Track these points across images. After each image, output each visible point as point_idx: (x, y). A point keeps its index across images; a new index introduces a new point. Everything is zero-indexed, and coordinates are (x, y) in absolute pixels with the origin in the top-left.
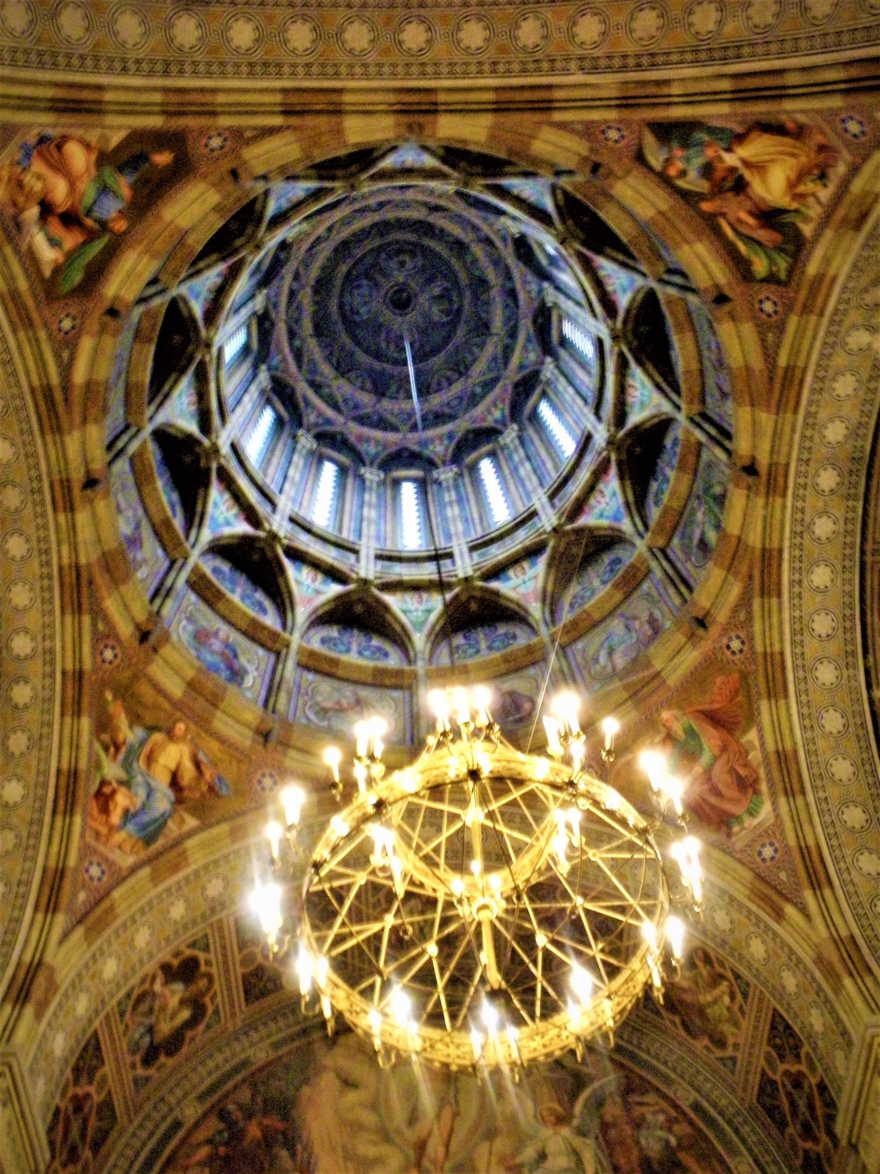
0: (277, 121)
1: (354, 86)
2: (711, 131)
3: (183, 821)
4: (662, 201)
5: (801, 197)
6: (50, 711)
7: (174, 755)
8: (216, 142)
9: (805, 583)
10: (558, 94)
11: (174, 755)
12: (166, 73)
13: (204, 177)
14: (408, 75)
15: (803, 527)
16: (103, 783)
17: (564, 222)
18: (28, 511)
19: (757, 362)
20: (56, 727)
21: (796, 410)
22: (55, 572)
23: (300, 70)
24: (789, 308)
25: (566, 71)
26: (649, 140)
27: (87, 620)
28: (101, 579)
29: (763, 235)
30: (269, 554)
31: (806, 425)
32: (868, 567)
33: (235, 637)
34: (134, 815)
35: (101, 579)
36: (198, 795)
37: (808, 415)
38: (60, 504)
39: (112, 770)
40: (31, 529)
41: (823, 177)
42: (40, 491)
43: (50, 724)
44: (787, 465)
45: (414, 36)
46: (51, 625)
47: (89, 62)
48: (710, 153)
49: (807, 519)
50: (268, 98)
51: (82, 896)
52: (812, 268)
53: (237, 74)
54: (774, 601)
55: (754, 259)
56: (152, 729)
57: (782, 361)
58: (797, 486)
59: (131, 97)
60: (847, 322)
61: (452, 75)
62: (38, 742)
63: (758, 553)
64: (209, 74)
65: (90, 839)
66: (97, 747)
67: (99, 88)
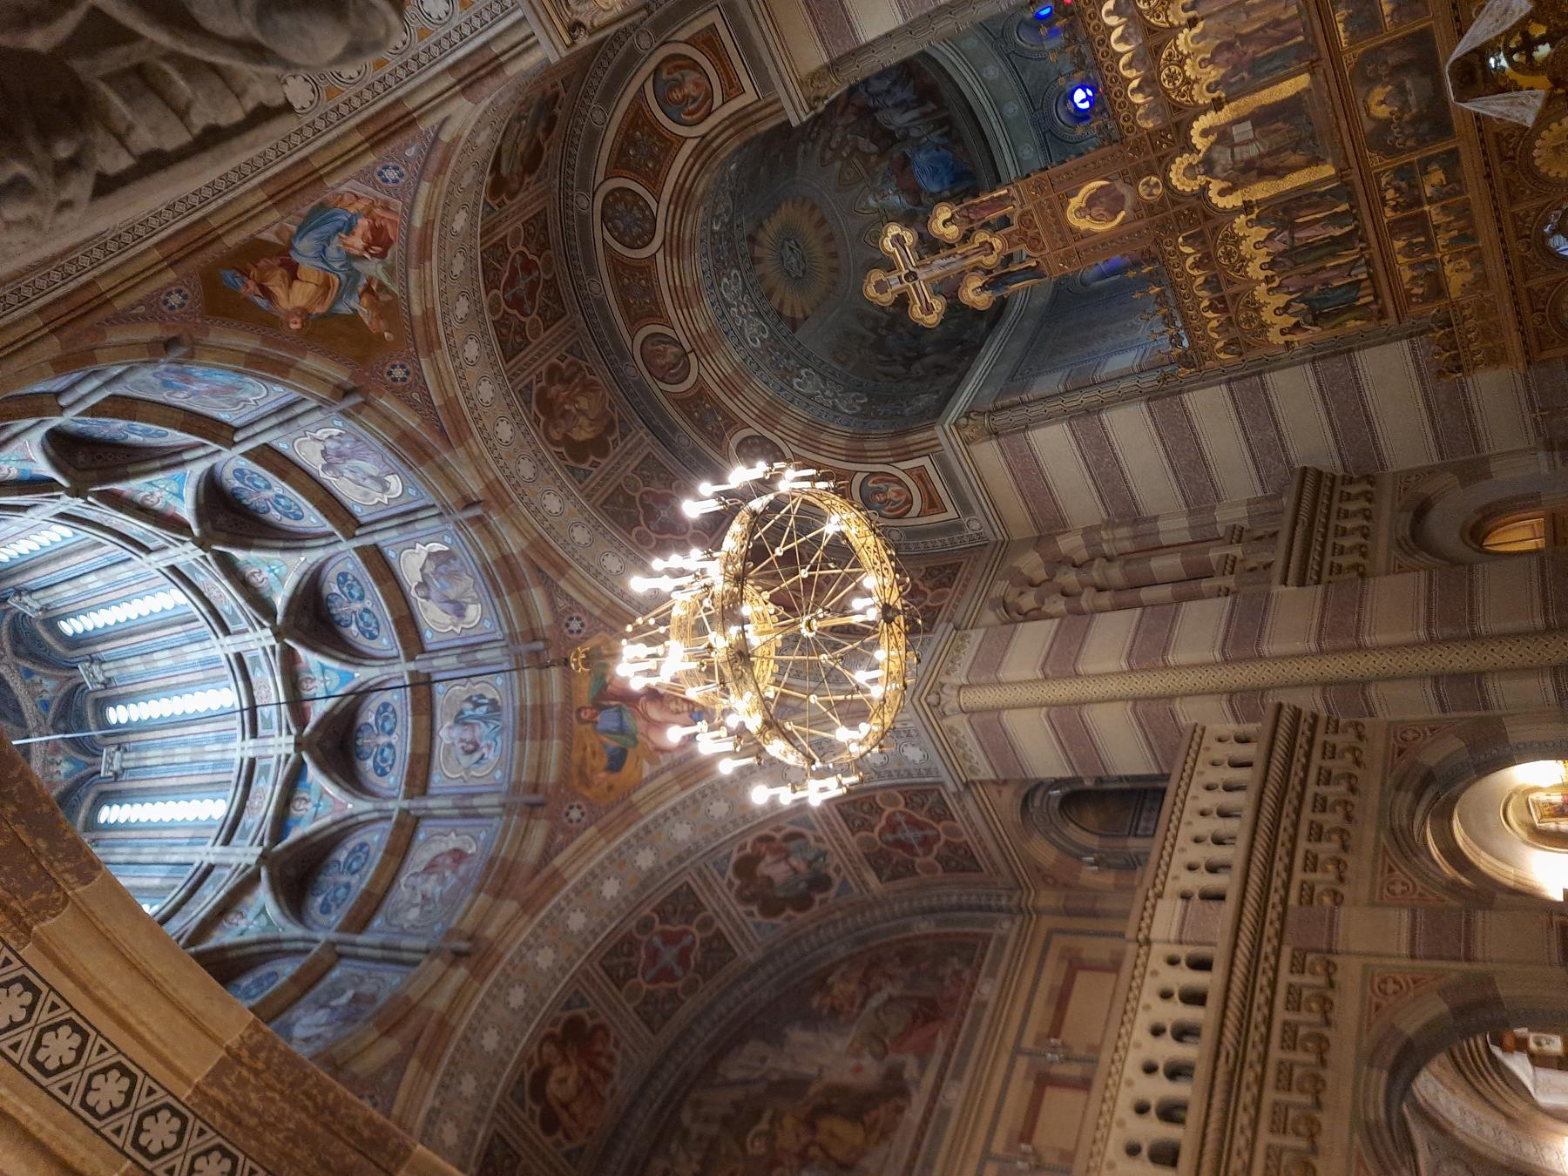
0: (558, 861)
1: (526, 929)
3: (277, 234)
6: (442, 303)
7: (296, 297)
8: (575, 814)
11: (296, 297)
12: (646, 829)
13: (557, 786)
16: (382, 255)
18: (512, 465)
20: (437, 293)
22: (473, 426)
23: (563, 903)
25: (437, 1094)
27: (437, 401)
28: (426, 436)
30: (71, 471)
33: (163, 396)
34: (340, 230)
35: (426, 436)
36: (262, 263)
38: (497, 486)
39: (373, 268)
40: (503, 451)
42: (514, 488)
43: (442, 293)
45: (517, 997)
46: (461, 379)
47: (699, 797)
50: (572, 869)
51: (410, 152)
53: (601, 865)
56: (331, 315)
59: (661, 798)
61: (483, 1005)
62: (446, 270)
64: (618, 850)
65: (398, 205)
66: (395, 289)
67: (683, 789)
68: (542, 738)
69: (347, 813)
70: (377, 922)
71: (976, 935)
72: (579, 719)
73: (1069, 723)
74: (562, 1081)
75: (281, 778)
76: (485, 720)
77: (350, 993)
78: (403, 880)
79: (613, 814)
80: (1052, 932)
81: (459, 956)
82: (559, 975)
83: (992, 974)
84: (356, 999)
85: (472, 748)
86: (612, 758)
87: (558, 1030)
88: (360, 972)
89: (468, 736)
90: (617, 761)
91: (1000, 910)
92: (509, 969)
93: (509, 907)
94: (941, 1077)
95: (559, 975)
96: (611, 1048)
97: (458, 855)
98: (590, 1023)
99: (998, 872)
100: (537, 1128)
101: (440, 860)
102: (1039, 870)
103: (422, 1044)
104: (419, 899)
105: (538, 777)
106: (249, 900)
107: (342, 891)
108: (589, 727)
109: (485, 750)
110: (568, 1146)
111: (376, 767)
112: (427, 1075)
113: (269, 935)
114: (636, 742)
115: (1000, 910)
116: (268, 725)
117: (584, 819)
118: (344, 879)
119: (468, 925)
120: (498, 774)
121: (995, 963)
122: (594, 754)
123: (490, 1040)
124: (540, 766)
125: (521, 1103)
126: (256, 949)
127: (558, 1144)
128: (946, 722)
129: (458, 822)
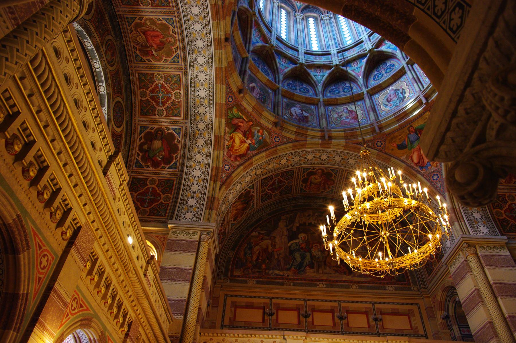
2: (255, 149)
4: (263, 121)
5: (231, 139)
8: (379, 144)
9: (202, 9)
10: (291, 149)
13: (385, 134)
14: (327, 151)
15: (206, 27)
17: (273, 54)
19: (230, 80)
21: (216, 68)
24: (226, 102)
25: (289, 153)
26: (268, 140)
29: (236, 121)
31: (212, 63)
32: (175, 8)
37: (212, 67)
41: (228, 148)
44: (215, 49)
45: (324, 157)
48: (254, 141)
49: (205, 30)
52: (223, 120)
54: (213, 3)
55: (237, 112)
57: (224, 86)
58: (211, 42)
60: (208, 100)
61: (316, 150)
63: (222, 19)
68: (397, 121)
69: (358, 78)
70: (330, 108)
71: (409, 280)
72: (409, 128)
73: (476, 297)
74: (316, 179)
75: (359, 53)
76: (399, 98)
77: (308, 115)
78: (345, 106)
79: (384, 155)
80: (418, 305)
81: (323, 137)
82: (336, 164)
83: (396, 289)
84: (306, 117)
85: (389, 100)
86: (402, 145)
87: (325, 171)
88: (315, 114)
89: (392, 96)
90: (401, 147)
91: (420, 286)
92: (329, 152)
93: (343, 142)
94: (358, 282)
95: (336, 164)
96: (331, 186)
97: (356, 117)
98: (333, 178)
99: (430, 282)
100: (302, 179)
101: (354, 113)
102: (435, 296)
103: (297, 143)
104: (340, 115)
105: (385, 127)
106: (325, 71)
107: (337, 92)
108: (408, 132)
109: (389, 105)
110: (303, 188)
111: (375, 76)
112: (291, 149)
113: (317, 83)
114: (411, 150)
115: (420, 286)
116: (373, 38)
117: (379, 147)
118: (341, 90)
119: (334, 134)
120: (383, 113)
121: (401, 289)
122: (400, 139)
123: (310, 157)
124: (388, 125)
125: (304, 172)
126: (313, 82)
127: (302, 186)
128: (461, 252)
129: (366, 111)
